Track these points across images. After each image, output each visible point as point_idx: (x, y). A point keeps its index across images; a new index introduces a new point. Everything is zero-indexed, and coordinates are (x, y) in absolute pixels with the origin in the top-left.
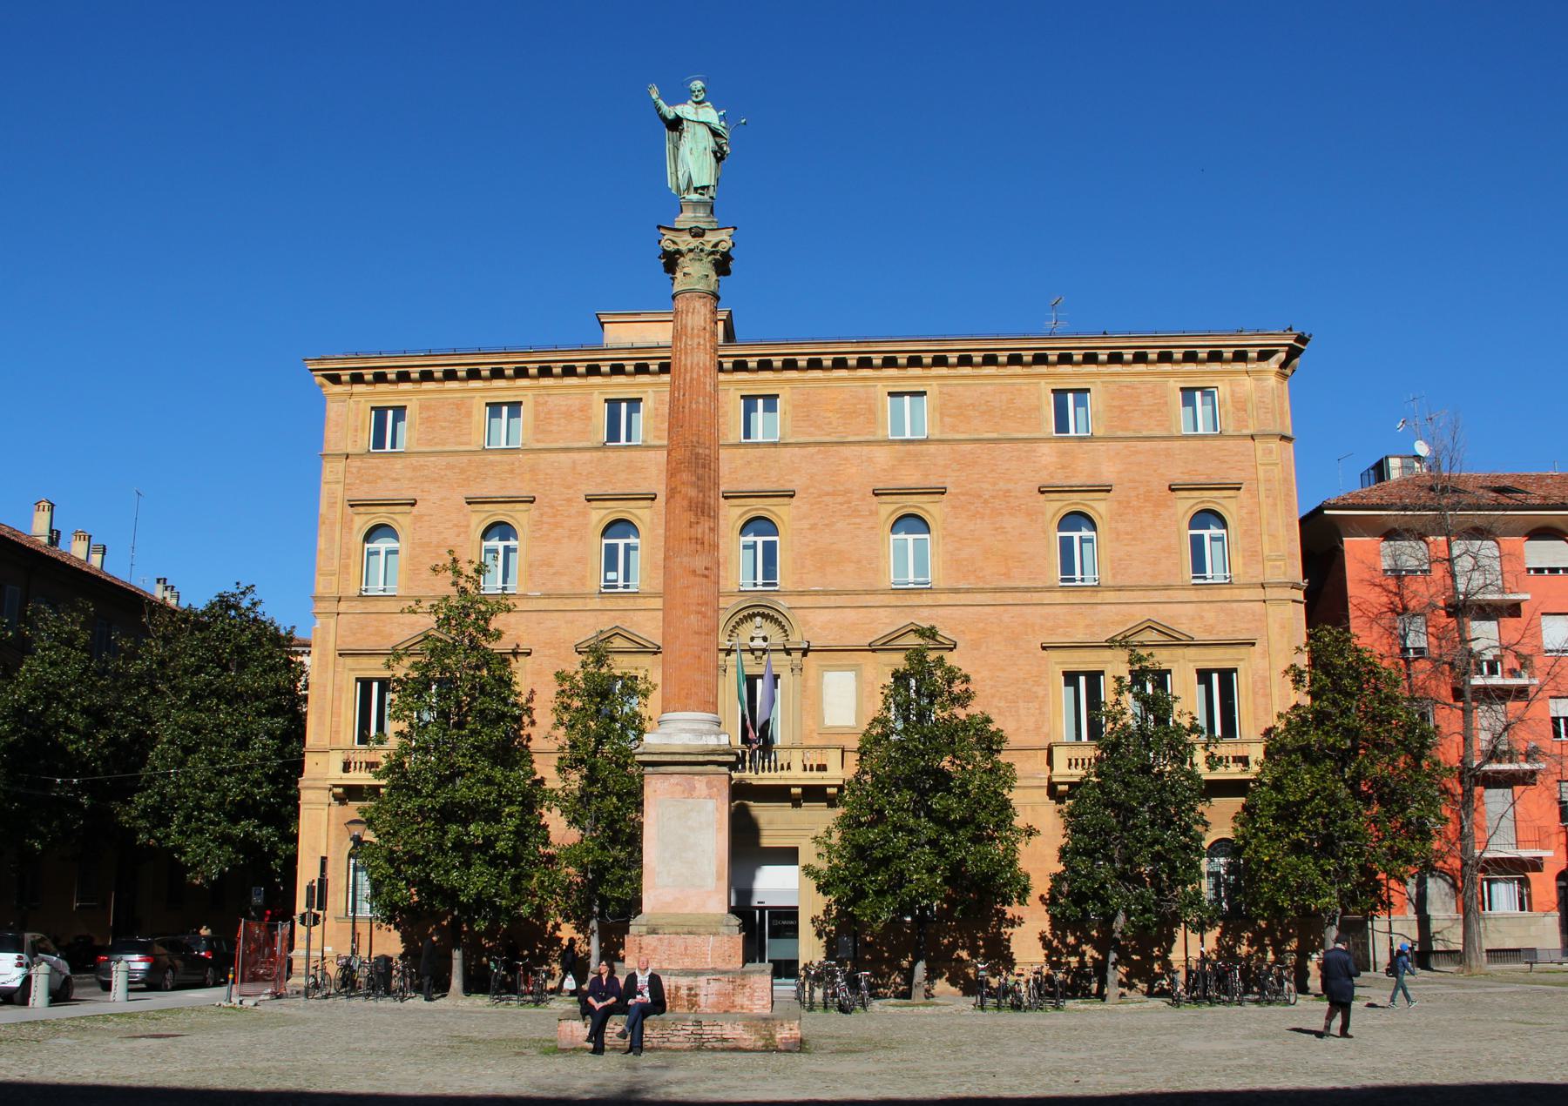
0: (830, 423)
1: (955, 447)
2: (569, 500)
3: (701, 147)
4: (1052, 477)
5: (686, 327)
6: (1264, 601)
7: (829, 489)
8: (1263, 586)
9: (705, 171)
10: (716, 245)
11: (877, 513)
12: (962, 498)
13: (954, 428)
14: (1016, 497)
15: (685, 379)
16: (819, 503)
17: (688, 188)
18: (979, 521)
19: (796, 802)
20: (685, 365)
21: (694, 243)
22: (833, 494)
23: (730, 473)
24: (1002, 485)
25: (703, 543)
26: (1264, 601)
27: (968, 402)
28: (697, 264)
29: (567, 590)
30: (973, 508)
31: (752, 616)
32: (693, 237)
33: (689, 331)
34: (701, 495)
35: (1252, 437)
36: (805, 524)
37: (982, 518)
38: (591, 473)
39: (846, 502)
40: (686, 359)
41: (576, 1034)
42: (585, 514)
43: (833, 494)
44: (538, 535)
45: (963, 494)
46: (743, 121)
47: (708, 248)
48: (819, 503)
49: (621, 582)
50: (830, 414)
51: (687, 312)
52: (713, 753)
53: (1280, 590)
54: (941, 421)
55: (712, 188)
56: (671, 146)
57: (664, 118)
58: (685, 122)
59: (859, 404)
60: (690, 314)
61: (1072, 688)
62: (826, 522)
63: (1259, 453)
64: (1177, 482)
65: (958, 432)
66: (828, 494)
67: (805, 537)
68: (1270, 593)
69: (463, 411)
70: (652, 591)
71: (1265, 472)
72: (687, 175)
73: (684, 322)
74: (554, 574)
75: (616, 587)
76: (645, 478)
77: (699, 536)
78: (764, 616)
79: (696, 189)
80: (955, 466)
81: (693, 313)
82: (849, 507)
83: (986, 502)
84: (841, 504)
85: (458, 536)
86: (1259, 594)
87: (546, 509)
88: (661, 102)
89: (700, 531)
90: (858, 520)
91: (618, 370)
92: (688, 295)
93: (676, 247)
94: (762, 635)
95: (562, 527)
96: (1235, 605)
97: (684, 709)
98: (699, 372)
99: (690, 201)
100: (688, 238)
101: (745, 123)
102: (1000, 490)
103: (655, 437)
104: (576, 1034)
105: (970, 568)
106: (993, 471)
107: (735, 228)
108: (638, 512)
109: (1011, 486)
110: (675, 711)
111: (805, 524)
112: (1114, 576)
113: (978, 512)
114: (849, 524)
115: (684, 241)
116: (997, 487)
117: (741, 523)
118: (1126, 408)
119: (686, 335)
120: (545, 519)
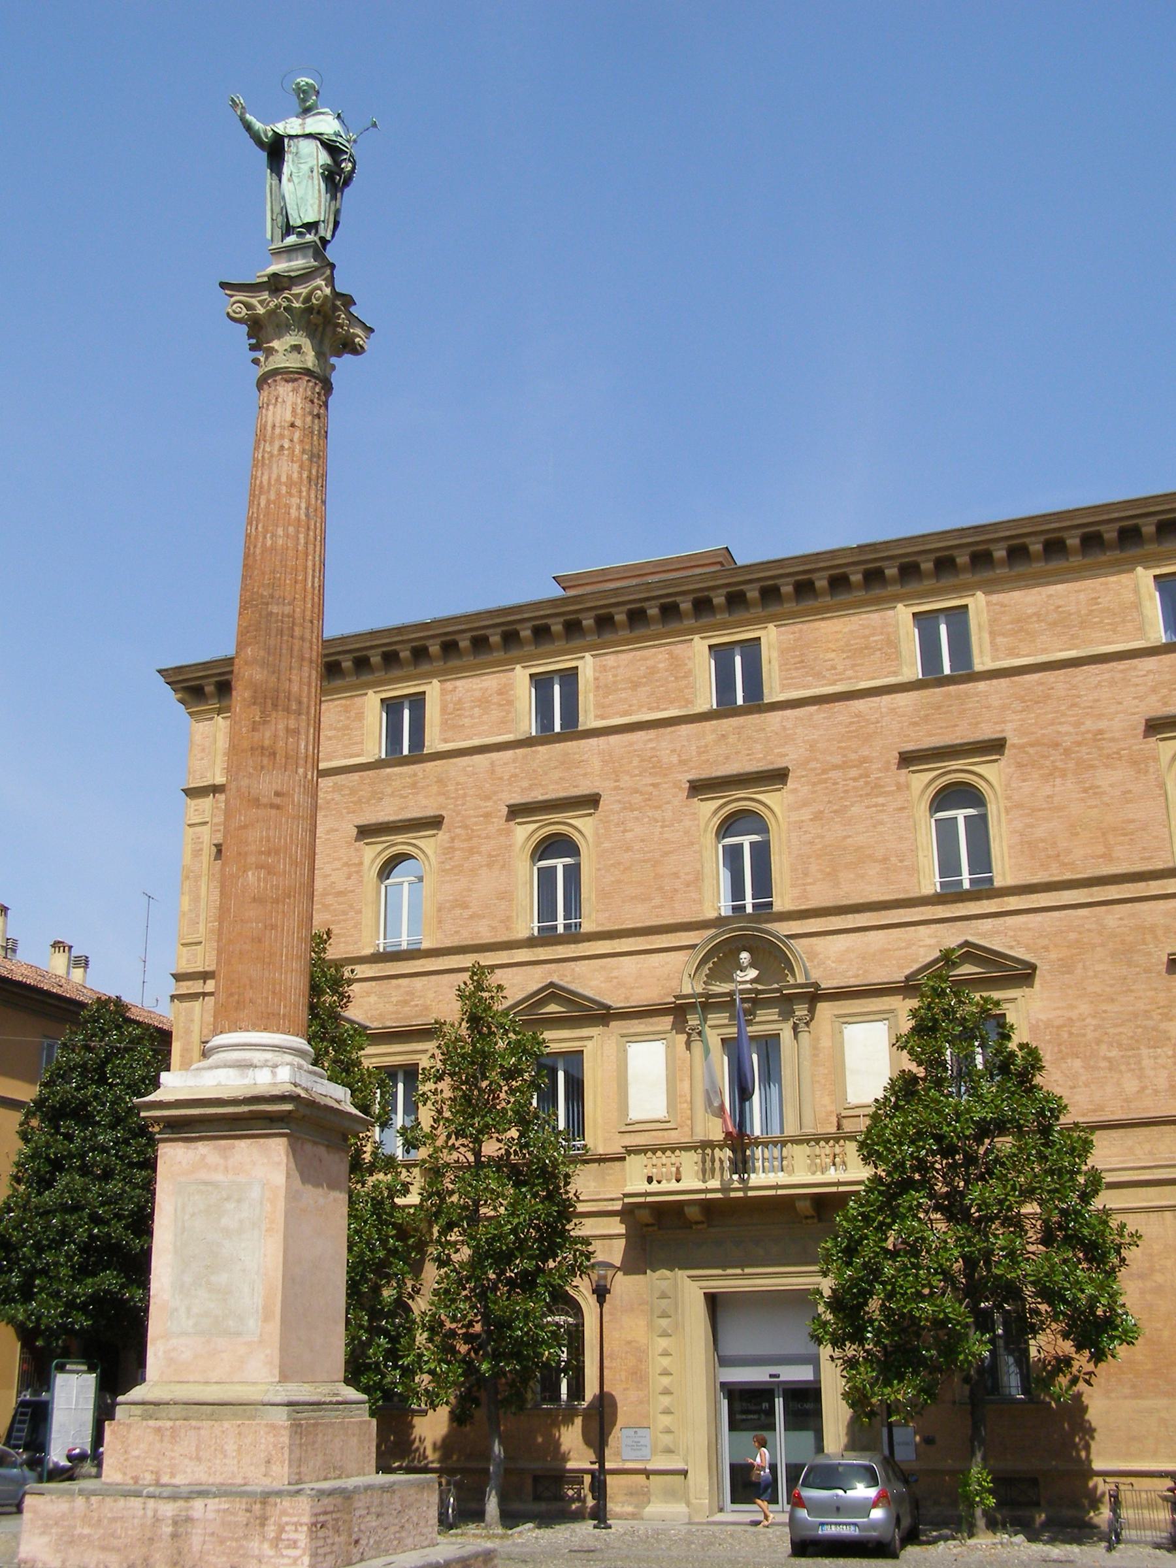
2: (487, 815)
3: (305, 168)
4: (1165, 704)
7: (837, 760)
11: (908, 786)
12: (1031, 750)
13: (1012, 653)
14: (1113, 740)
16: (825, 781)
18: (1058, 781)
22: (843, 766)
23: (699, 754)
24: (1089, 724)
25: (274, 754)
29: (487, 937)
30: (1048, 763)
34: (274, 679)
36: (806, 814)
37: (1063, 776)
38: (516, 776)
39: (861, 776)
42: (509, 833)
43: (843, 766)
44: (448, 867)
45: (1032, 745)
48: (825, 781)
50: (832, 655)
54: (993, 643)
59: (873, 635)
60: (271, 407)
65: (1018, 656)
66: (835, 767)
69: (352, 714)
70: (599, 929)
74: (471, 917)
76: (585, 775)
77: (267, 743)
80: (1017, 705)
82: (867, 783)
84: (854, 779)
85: (349, 878)
87: (458, 831)
89: (268, 734)
90: (881, 800)
95: (479, 853)
102: (1088, 732)
103: (596, 716)
105: (1050, 853)
106: (1074, 705)
109: (1103, 724)
111: (806, 814)
113: (1056, 768)
114: (868, 807)
116: (1083, 728)
117: (716, 821)
120: (457, 844)
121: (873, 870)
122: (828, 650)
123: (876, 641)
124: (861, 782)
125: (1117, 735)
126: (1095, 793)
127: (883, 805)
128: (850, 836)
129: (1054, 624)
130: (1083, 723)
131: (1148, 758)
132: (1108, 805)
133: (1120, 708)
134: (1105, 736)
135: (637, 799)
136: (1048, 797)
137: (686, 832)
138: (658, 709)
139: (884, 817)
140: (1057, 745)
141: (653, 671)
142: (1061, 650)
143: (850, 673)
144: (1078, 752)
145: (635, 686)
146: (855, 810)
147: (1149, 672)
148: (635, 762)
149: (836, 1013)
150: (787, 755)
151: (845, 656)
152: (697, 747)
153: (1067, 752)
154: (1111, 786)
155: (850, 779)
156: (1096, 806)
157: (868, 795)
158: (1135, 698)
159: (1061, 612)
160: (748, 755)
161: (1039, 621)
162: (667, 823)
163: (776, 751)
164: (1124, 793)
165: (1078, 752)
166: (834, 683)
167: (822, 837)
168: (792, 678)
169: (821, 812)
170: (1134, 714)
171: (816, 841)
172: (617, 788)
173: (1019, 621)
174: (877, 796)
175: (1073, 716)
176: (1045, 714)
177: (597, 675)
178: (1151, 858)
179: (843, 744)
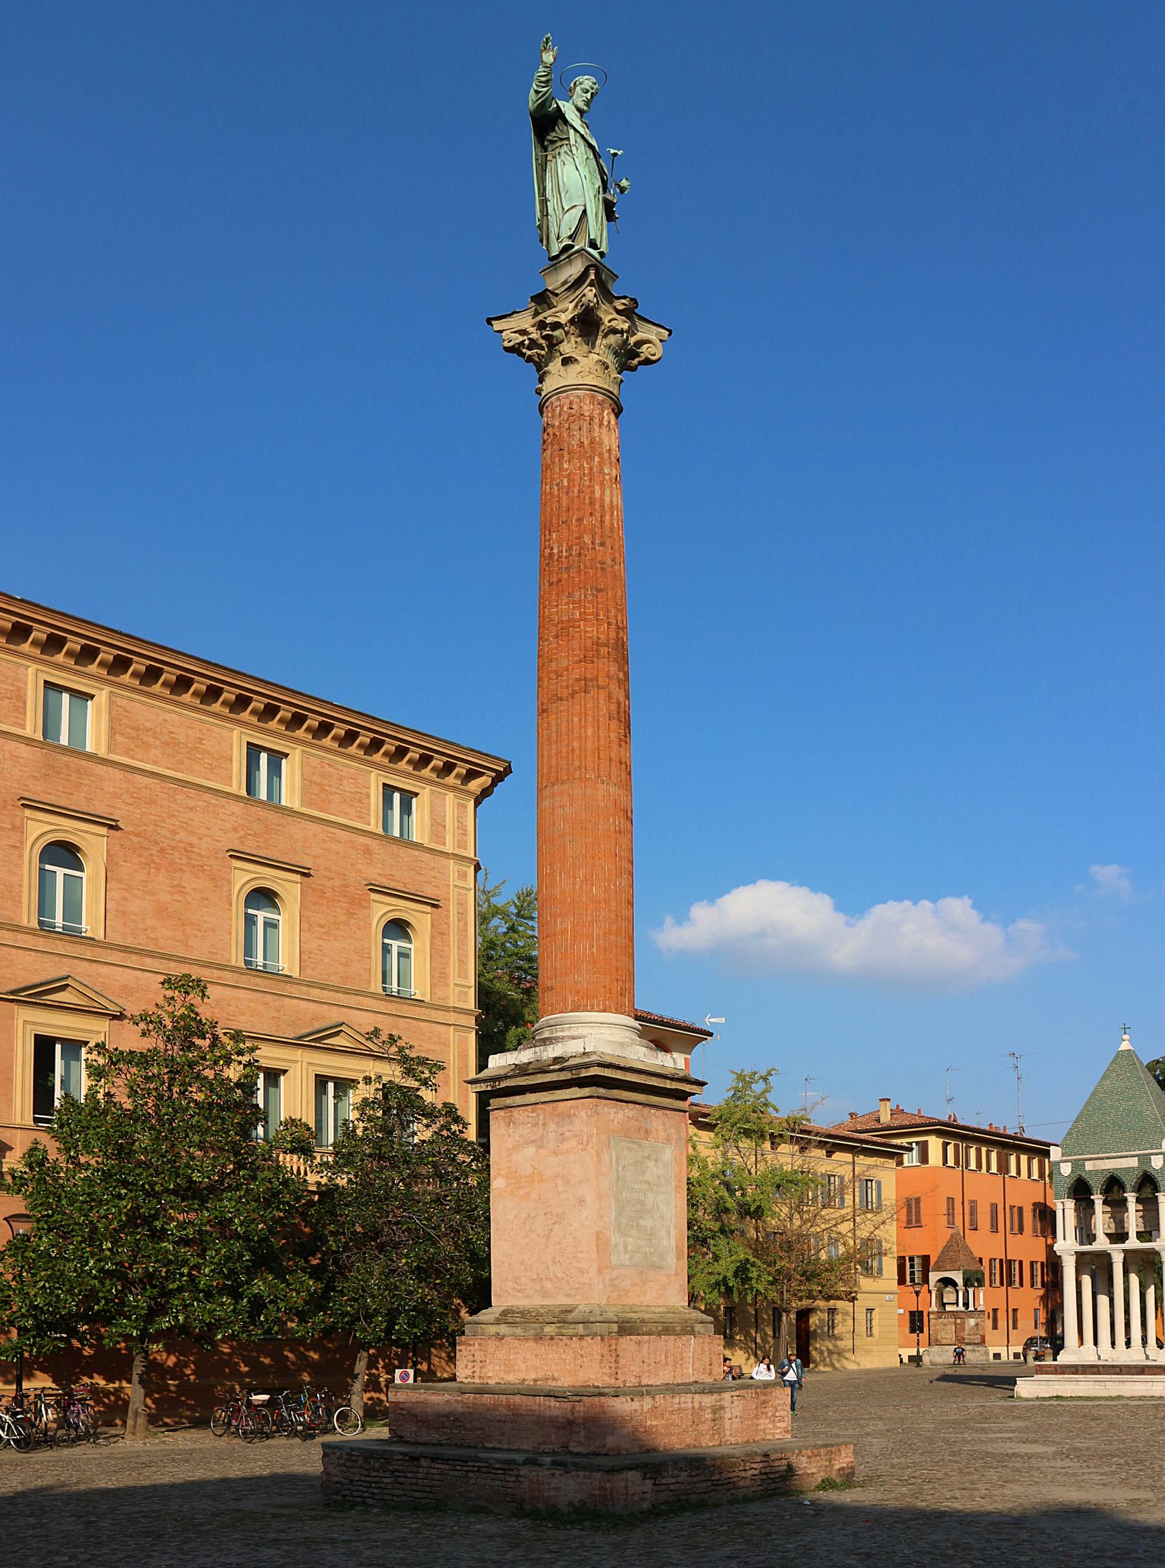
24: (182, 835)
27: (148, 725)
37: (158, 869)
41: (632, 1491)
80: (126, 796)
83: (162, 850)
102: (181, 841)
104: (632, 1491)
109: (194, 840)
113: (154, 862)
116: (177, 837)
125: (203, 853)
126: (180, 891)
129: (166, 744)
130: (178, 834)
131: (224, 879)
132: (189, 903)
133: (208, 832)
136: (143, 881)
140: (156, 842)
142: (169, 768)
144: (171, 854)
153: (162, 850)
156: (179, 901)
159: (174, 738)
165: (171, 854)
175: (169, 824)
176: (150, 814)
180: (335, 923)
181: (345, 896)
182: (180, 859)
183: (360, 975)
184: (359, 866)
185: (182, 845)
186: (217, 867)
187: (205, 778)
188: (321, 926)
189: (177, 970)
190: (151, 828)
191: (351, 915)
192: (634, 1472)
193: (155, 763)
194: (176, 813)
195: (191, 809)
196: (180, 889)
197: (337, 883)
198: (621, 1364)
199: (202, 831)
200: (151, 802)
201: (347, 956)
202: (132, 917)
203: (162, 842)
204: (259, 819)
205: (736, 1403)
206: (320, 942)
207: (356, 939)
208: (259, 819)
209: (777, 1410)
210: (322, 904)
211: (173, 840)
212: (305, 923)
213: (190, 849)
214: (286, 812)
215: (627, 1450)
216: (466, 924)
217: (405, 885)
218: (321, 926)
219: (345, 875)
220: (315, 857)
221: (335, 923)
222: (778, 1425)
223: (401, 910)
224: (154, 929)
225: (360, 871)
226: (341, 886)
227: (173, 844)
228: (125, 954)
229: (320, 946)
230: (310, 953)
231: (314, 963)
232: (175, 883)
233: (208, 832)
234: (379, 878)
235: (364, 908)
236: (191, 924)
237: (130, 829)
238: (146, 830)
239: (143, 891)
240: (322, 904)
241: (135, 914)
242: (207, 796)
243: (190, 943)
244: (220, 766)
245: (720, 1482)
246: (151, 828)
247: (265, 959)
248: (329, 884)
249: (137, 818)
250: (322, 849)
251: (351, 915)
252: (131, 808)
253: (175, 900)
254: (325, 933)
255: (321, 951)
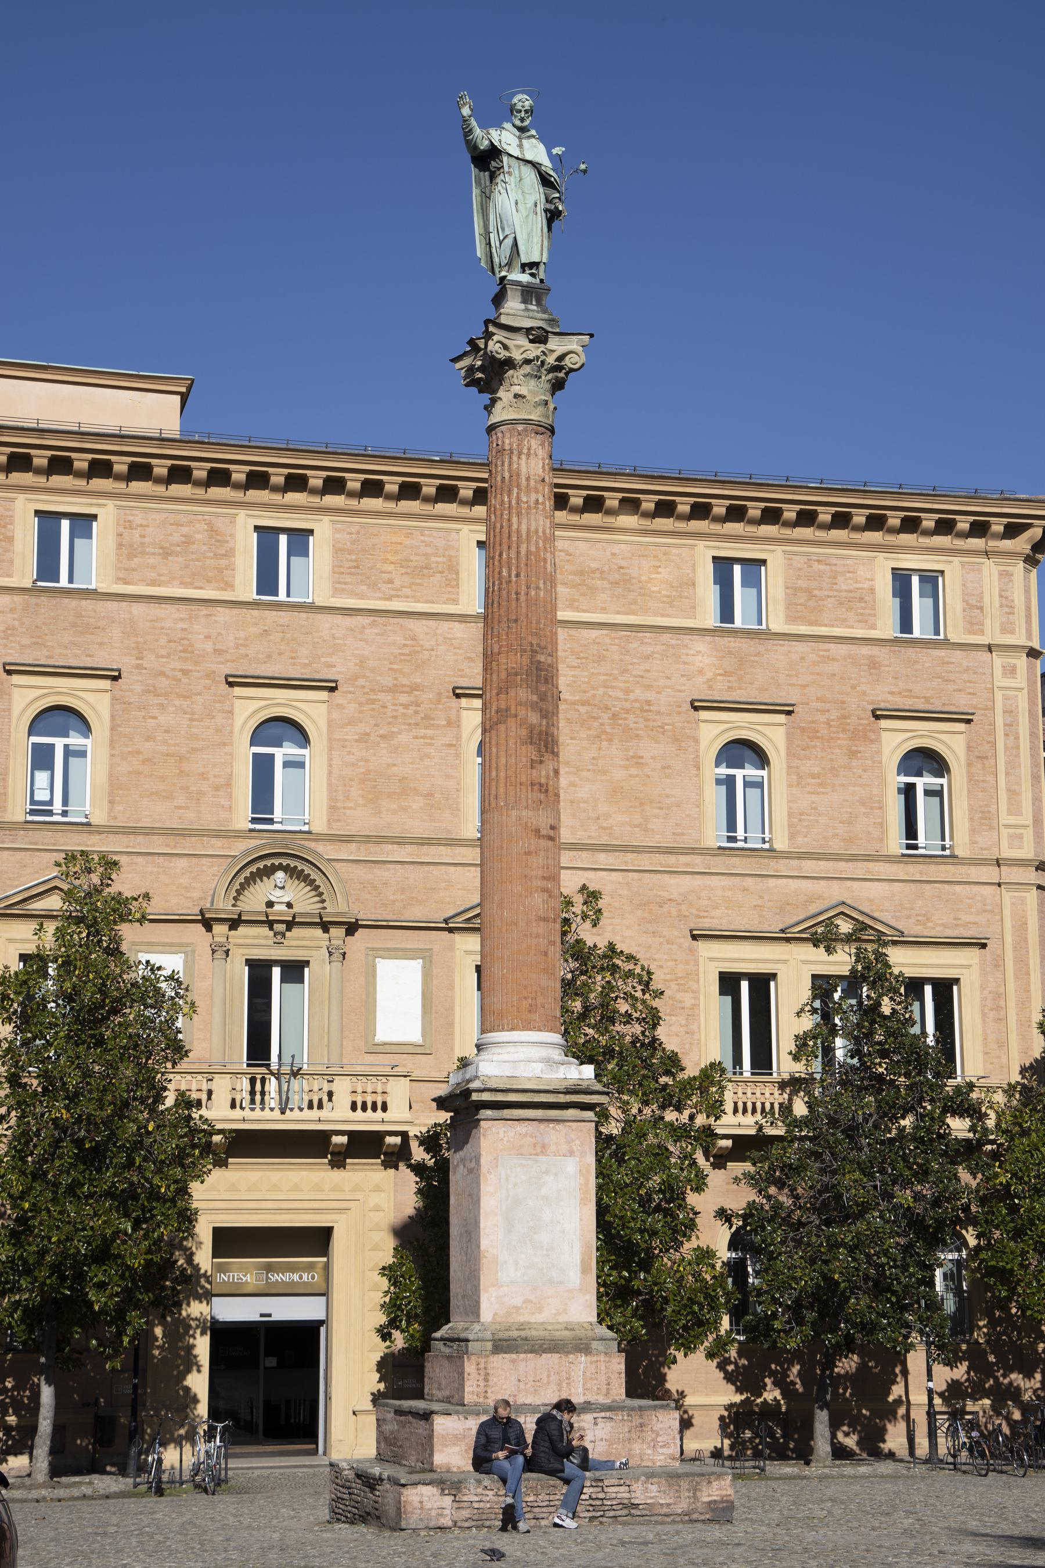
0: (390, 581)
1: (572, 632)
3: (531, 204)
4: (710, 687)
5: (518, 475)
6: (999, 885)
7: (387, 681)
8: (998, 863)
9: (535, 240)
10: (560, 358)
12: (583, 709)
14: (659, 713)
15: (518, 553)
16: (373, 702)
17: (509, 264)
19: (338, 1160)
20: (518, 531)
21: (534, 351)
22: (393, 690)
23: (238, 646)
24: (638, 693)
25: (547, 791)
26: (999, 885)
28: (533, 382)
31: (269, 871)
32: (531, 341)
33: (524, 482)
34: (544, 722)
35: (990, 648)
36: (350, 733)
37: (610, 740)
38: (14, 629)
39: (412, 703)
40: (519, 523)
43: (393, 690)
46: (583, 167)
47: (551, 360)
48: (373, 702)
49: (57, 806)
50: (391, 568)
51: (520, 454)
52: (568, 1092)
53: (1021, 869)
55: (542, 267)
56: (478, 191)
57: (472, 147)
58: (505, 159)
59: (435, 555)
60: (524, 457)
61: (729, 998)
62: (382, 732)
63: (998, 671)
64: (882, 705)
65: (578, 610)
67: (349, 753)
68: (1009, 874)
71: (1006, 698)
72: (509, 242)
73: (515, 466)
75: (50, 813)
76: (101, 644)
77: (543, 781)
78: (286, 869)
79: (524, 267)
81: (528, 455)
82: (416, 712)
84: (406, 706)
86: (991, 874)
88: (473, 122)
89: (543, 773)
90: (429, 732)
91: (60, 465)
92: (520, 428)
93: (507, 354)
94: (286, 899)
96: (958, 888)
97: (527, 1027)
98: (537, 543)
99: (518, 283)
100: (522, 341)
101: (585, 171)
102: (637, 701)
105: (591, 815)
106: (626, 671)
107: (591, 336)
108: (89, 697)
109: (651, 695)
110: (512, 1029)
111: (350, 733)
112: (792, 836)
113: (605, 732)
114: (416, 737)
115: (518, 347)
116: (632, 696)
118: (816, 592)
119: (518, 486)
121: (417, 804)
122: (385, 561)
123: (437, 563)
124: (411, 711)
125: (663, 709)
127: (432, 738)
128: (394, 765)
130: (633, 691)
132: (648, 776)
133: (668, 682)
134: (652, 708)
135: (163, 683)
136: (594, 758)
137: (218, 731)
138: (191, 585)
139: (431, 750)
140: (607, 708)
141: (188, 540)
143: (407, 591)
144: (625, 719)
145: (166, 554)
146: (402, 738)
147: (700, 652)
148: (163, 641)
149: (370, 945)
150: (335, 666)
151: (403, 570)
152: (236, 638)
153: (614, 717)
154: (652, 758)
155: (401, 705)
156: (637, 776)
157: (417, 724)
158: (682, 676)
160: (292, 658)
161: (602, 579)
162: (196, 717)
163: (323, 659)
164: (664, 768)
165: (625, 719)
166: (389, 599)
167: (367, 761)
168: (345, 583)
169: (367, 734)
170: (681, 691)
171: (360, 764)
172: (139, 667)
173: (582, 573)
174: (426, 728)
177: (121, 530)
178: (683, 834)
179: (395, 666)
180: (833, 768)
181: (844, 731)
182: (635, 723)
183: (869, 833)
184: (863, 688)
185: (637, 705)
186: (680, 725)
187: (663, 615)
188: (813, 776)
189: (636, 862)
190: (601, 691)
191: (853, 754)
192: (429, 1488)
193: (603, 610)
194: (630, 667)
195: (648, 657)
196: (637, 761)
197: (834, 714)
198: (490, 1383)
199: (662, 682)
200: (600, 659)
201: (850, 810)
202: (582, 805)
203: (614, 706)
204: (730, 653)
205: (601, 1425)
206: (814, 798)
207: (861, 785)
208: (730, 653)
209: (658, 1435)
210: (814, 747)
211: (626, 700)
212: (797, 778)
213: (647, 708)
214: (763, 636)
215: (459, 1468)
216: (1017, 738)
217: (927, 700)
218: (813, 776)
219: (843, 703)
220: (803, 687)
221: (833, 768)
222: (661, 1451)
223: (922, 736)
224: (607, 816)
225: (864, 693)
226: (838, 718)
227: (627, 705)
228: (575, 853)
229: (813, 802)
230: (802, 814)
231: (806, 827)
232: (631, 754)
233: (668, 682)
234: (890, 698)
235: (872, 741)
236: (651, 802)
237: (577, 698)
238: (594, 696)
239: (594, 771)
240: (814, 747)
241: (584, 802)
242: (666, 637)
243: (650, 826)
244: (680, 597)
245: (536, 1504)
246: (601, 691)
247: (746, 832)
248: (823, 718)
249: (585, 683)
250: (812, 674)
251: (853, 754)
252: (577, 672)
253: (631, 776)
254: (820, 785)
255: (816, 809)
